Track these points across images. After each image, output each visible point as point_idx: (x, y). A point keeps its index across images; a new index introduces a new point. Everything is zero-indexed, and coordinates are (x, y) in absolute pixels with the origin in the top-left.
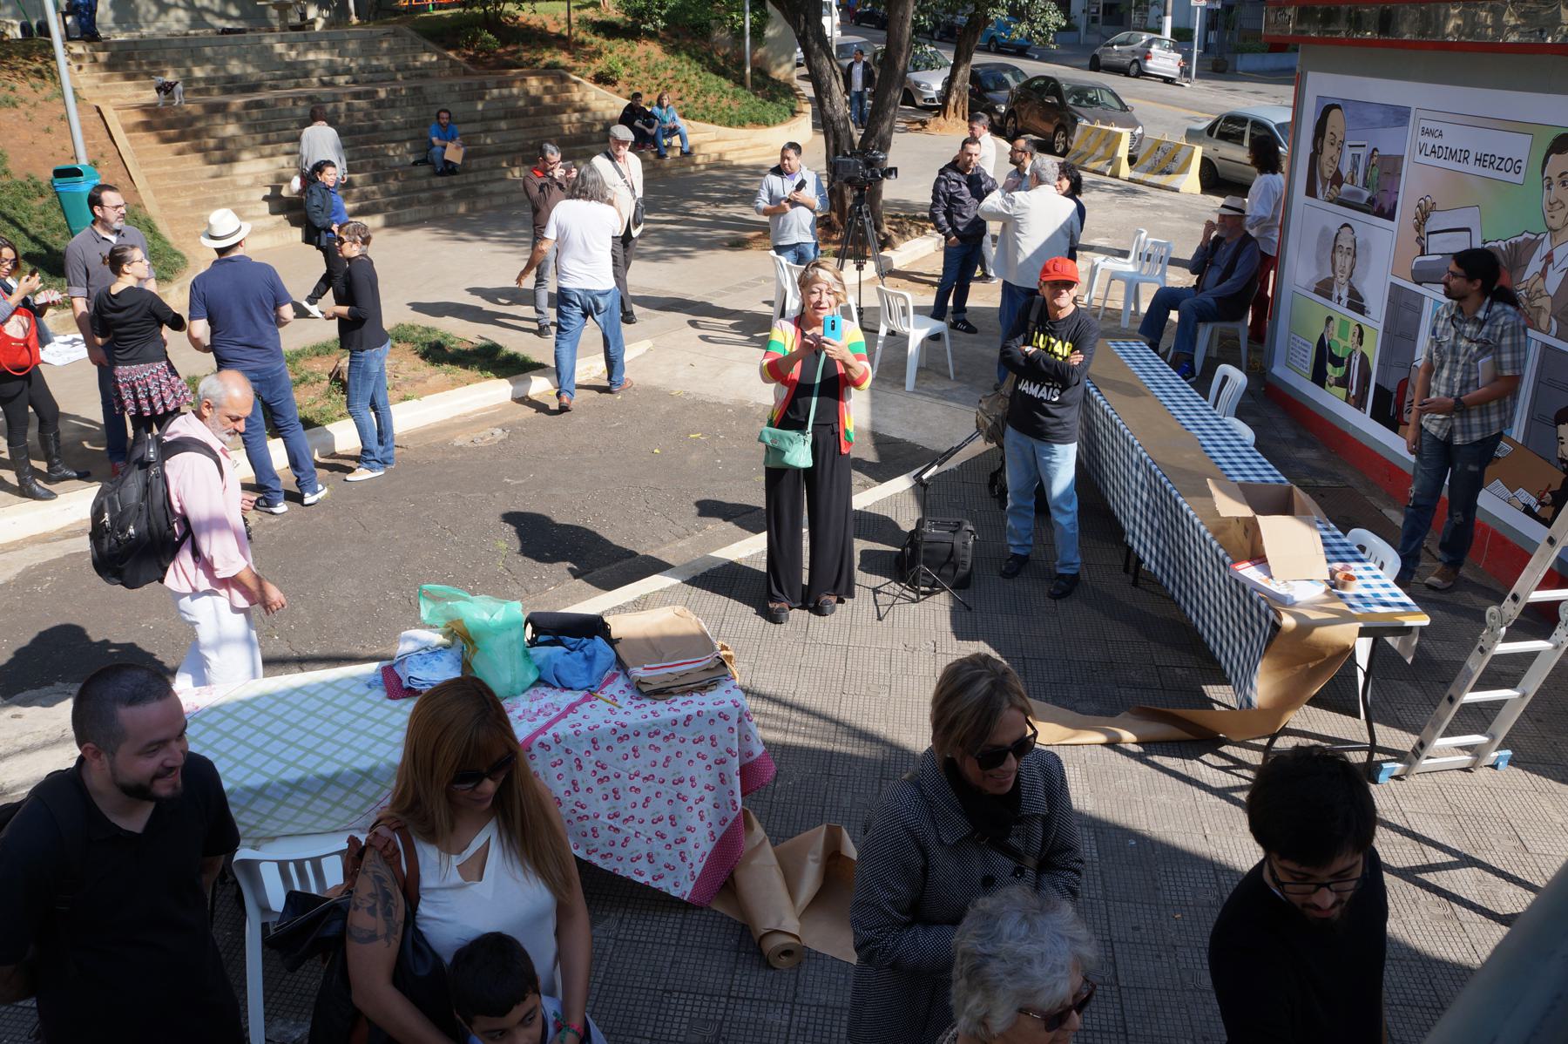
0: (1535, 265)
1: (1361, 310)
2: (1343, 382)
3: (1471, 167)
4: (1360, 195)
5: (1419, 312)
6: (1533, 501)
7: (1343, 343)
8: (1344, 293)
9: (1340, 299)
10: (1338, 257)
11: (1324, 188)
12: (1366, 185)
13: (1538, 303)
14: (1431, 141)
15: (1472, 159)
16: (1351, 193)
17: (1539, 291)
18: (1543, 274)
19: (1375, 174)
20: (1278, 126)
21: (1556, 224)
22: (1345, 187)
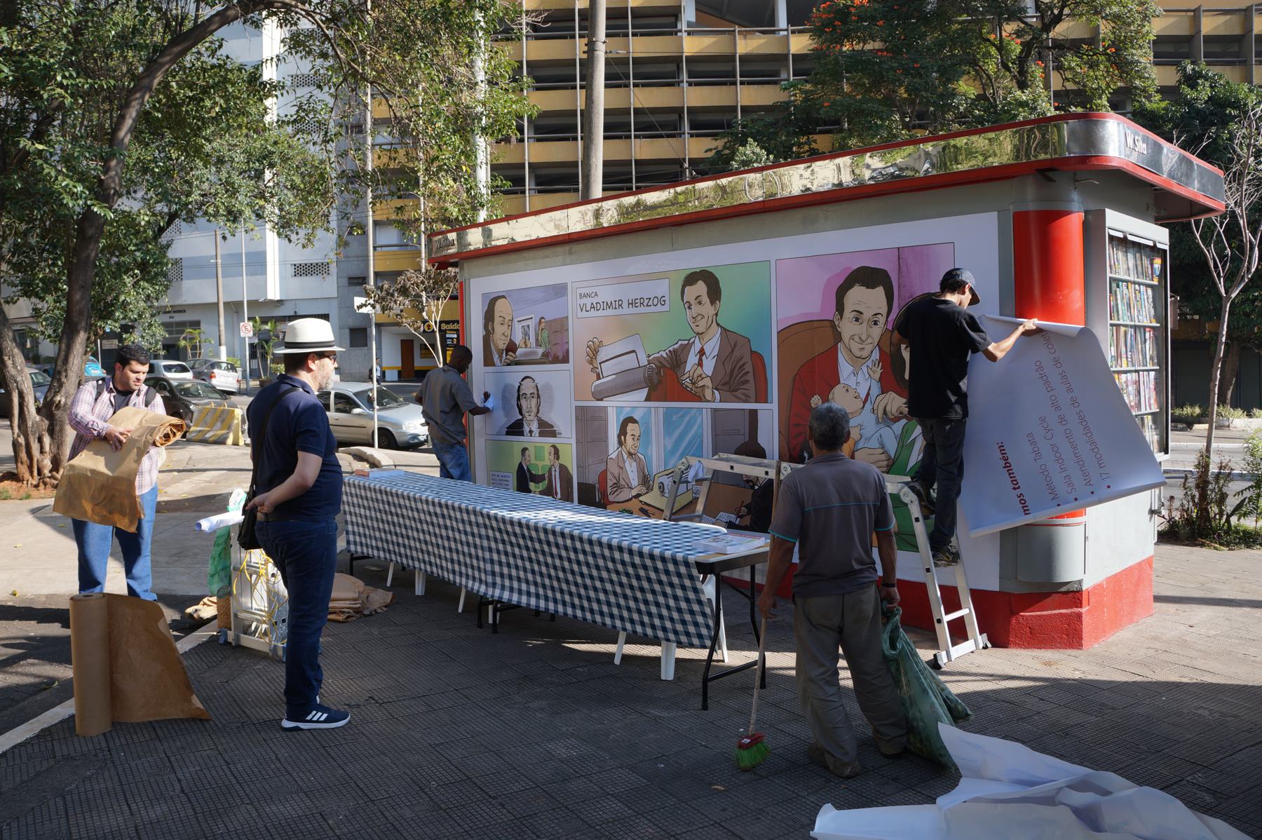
0: (692, 359)
1: (553, 434)
2: (549, 492)
3: (626, 310)
4: (535, 353)
5: (606, 421)
6: (733, 518)
7: (540, 464)
8: (535, 426)
9: (531, 432)
10: (523, 403)
11: (500, 357)
12: (538, 344)
13: (700, 384)
14: (588, 301)
15: (625, 305)
16: (526, 354)
18: (700, 364)
19: (546, 334)
20: (355, 394)
21: (700, 330)
22: (519, 351)
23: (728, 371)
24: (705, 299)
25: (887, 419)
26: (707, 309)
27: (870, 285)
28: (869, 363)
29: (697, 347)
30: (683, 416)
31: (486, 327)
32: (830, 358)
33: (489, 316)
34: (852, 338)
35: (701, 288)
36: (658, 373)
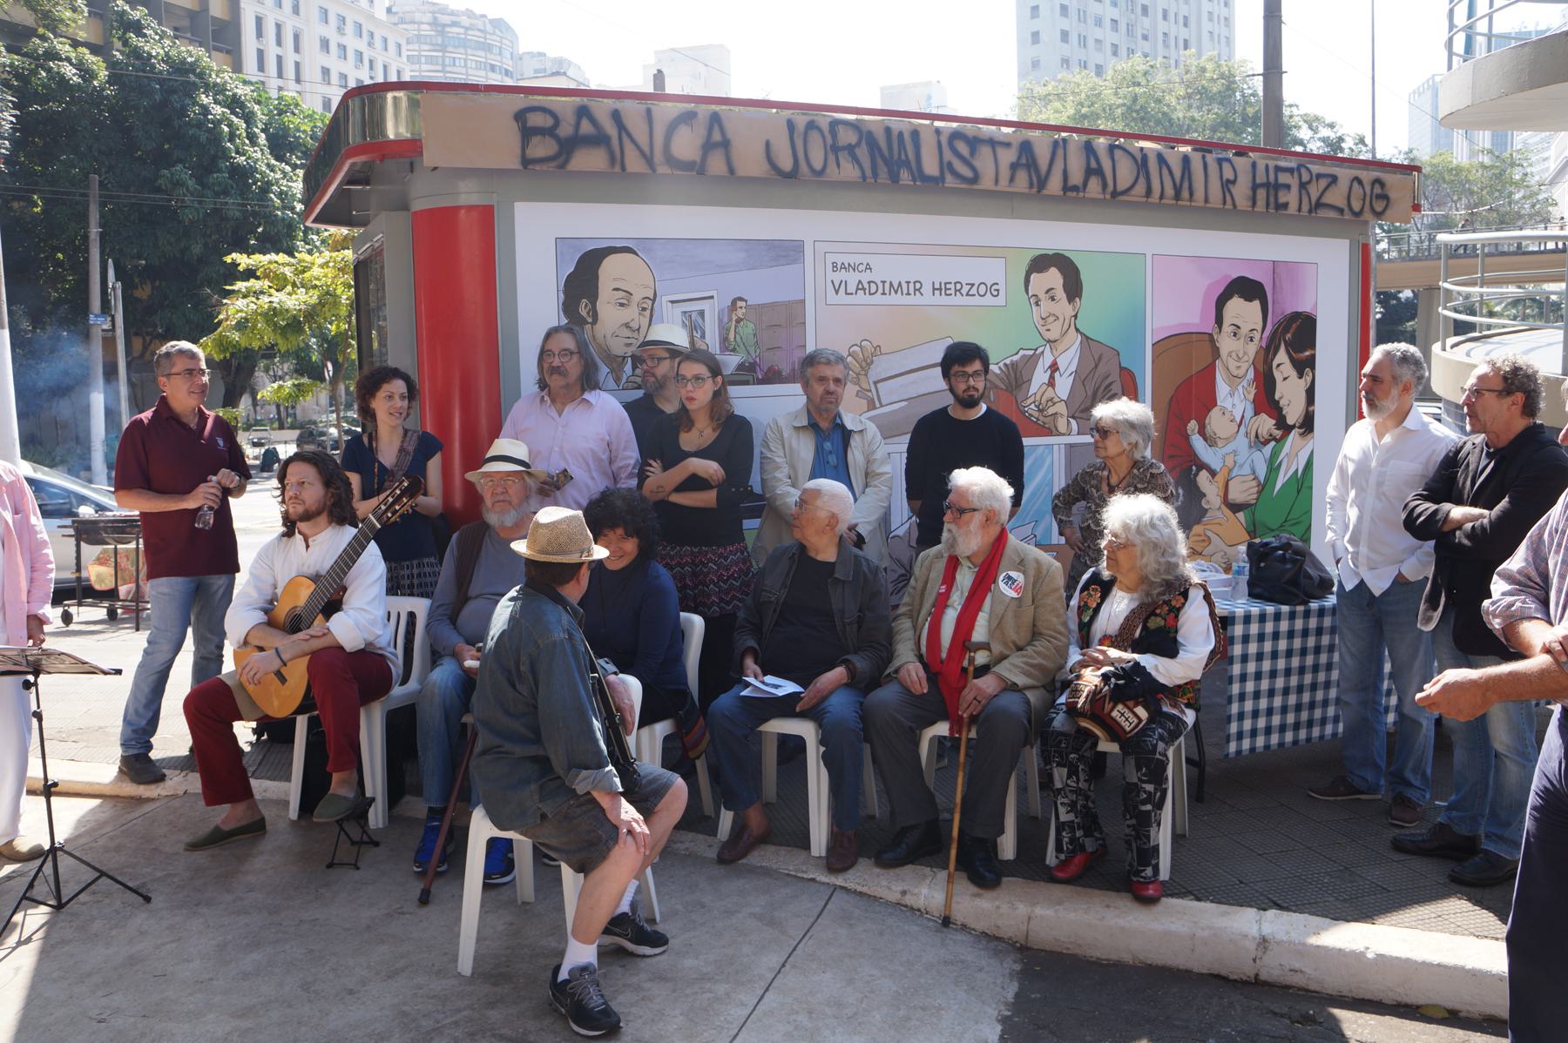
3: (927, 298)
11: (616, 373)
13: (1051, 411)
14: (852, 278)
15: (927, 289)
18: (1051, 383)
19: (748, 329)
21: (1052, 336)
24: (1060, 293)
25: (1259, 442)
26: (1063, 308)
27: (1249, 299)
28: (1245, 383)
29: (1048, 359)
31: (569, 307)
32: (1209, 374)
34: (1230, 354)
35: (1054, 277)
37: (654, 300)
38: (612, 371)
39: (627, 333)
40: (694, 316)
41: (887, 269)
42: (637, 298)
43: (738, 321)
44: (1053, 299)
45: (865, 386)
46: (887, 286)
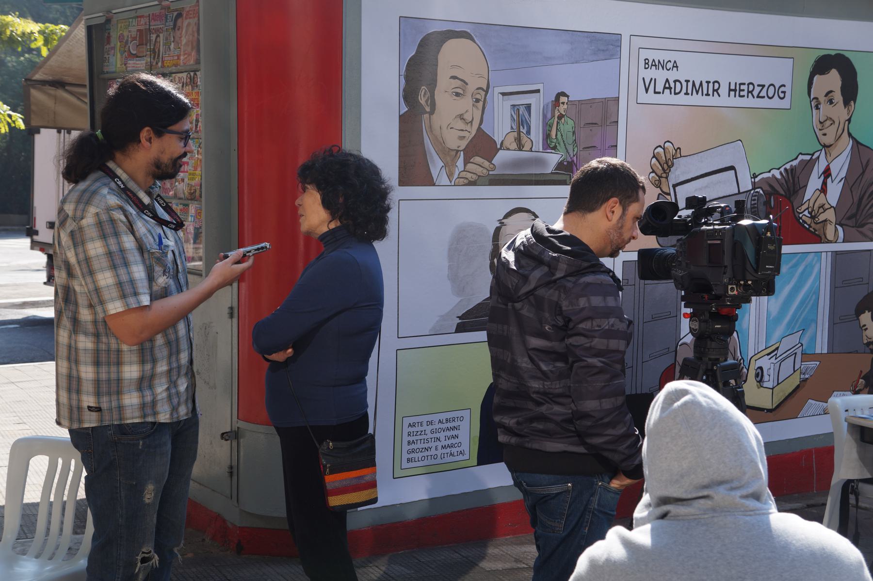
0: (814, 183)
3: (724, 99)
4: (540, 162)
11: (449, 167)
12: (549, 144)
13: (822, 218)
14: (661, 76)
15: (724, 90)
16: (517, 163)
17: (822, 206)
18: (824, 189)
19: (568, 125)
21: (827, 140)
22: (502, 156)
23: (856, 199)
24: (838, 97)
26: (839, 112)
30: (796, 266)
31: (409, 95)
33: (418, 74)
35: (833, 80)
36: (767, 203)
37: (487, 92)
38: (446, 165)
39: (460, 125)
40: (522, 109)
41: (694, 68)
42: (471, 88)
43: (561, 117)
44: (831, 102)
45: (666, 190)
46: (690, 84)
